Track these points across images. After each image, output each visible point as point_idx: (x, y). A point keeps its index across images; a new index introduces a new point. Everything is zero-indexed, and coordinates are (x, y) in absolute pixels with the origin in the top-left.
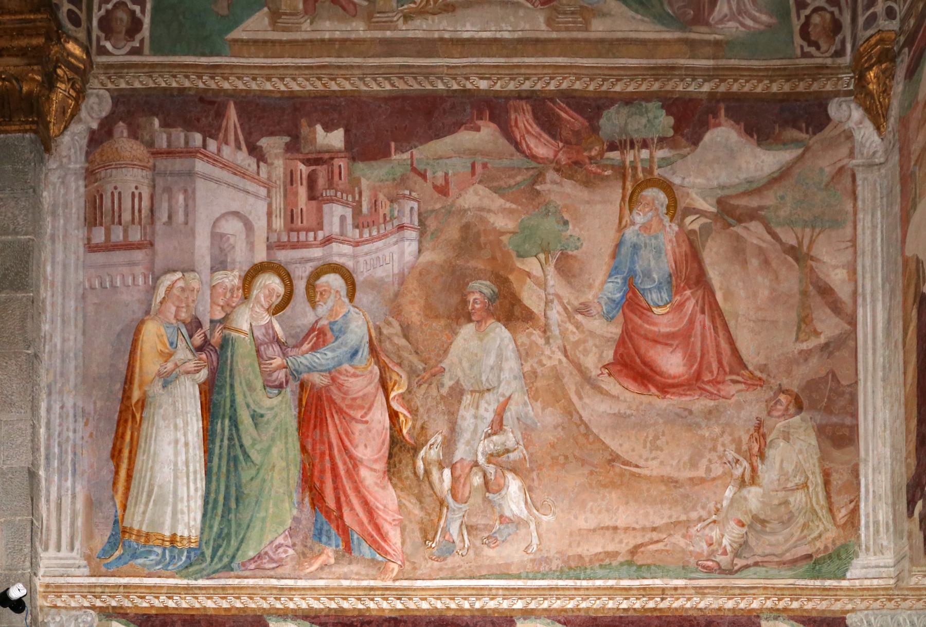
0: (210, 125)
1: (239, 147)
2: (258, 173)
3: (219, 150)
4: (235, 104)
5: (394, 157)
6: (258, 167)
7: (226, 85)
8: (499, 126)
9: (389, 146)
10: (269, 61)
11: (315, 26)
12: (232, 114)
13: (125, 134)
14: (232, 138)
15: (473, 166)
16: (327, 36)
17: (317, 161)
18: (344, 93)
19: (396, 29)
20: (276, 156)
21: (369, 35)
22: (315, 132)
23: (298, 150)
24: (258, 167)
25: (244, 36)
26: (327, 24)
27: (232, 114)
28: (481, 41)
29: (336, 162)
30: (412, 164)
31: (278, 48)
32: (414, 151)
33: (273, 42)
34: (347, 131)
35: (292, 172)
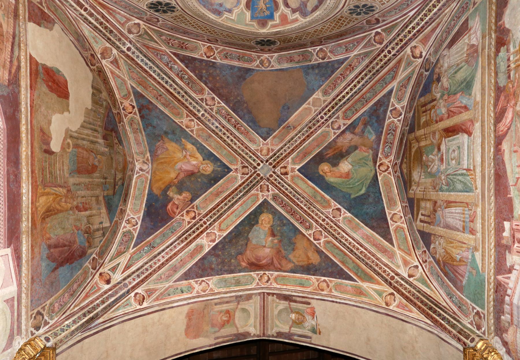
0: (503, 290)
1: (509, 278)
2: (518, 270)
3: (510, 289)
4: (497, 275)
5: (512, 196)
6: (515, 269)
7: (492, 278)
8: (502, 140)
9: (509, 198)
10: (487, 255)
11: (478, 231)
12: (500, 277)
13: (506, 335)
14: (506, 280)
15: (515, 152)
16: (481, 226)
17: (514, 237)
18: (495, 219)
19: (479, 193)
20: (512, 259)
21: (480, 206)
22: (505, 237)
23: (510, 247)
24: (515, 269)
25: (481, 265)
26: (478, 225)
27: (500, 277)
28: (482, 153)
29: (514, 227)
30: (514, 185)
31: (483, 250)
32: (510, 184)
33: (482, 252)
34: (505, 220)
35: (517, 252)
